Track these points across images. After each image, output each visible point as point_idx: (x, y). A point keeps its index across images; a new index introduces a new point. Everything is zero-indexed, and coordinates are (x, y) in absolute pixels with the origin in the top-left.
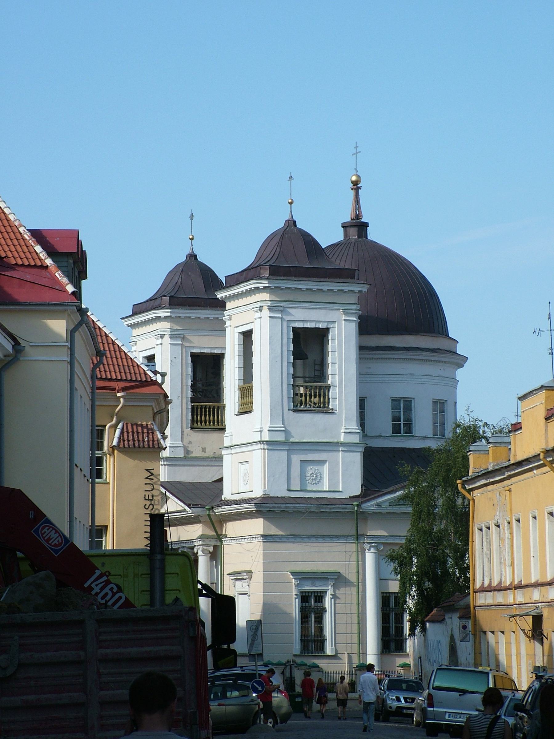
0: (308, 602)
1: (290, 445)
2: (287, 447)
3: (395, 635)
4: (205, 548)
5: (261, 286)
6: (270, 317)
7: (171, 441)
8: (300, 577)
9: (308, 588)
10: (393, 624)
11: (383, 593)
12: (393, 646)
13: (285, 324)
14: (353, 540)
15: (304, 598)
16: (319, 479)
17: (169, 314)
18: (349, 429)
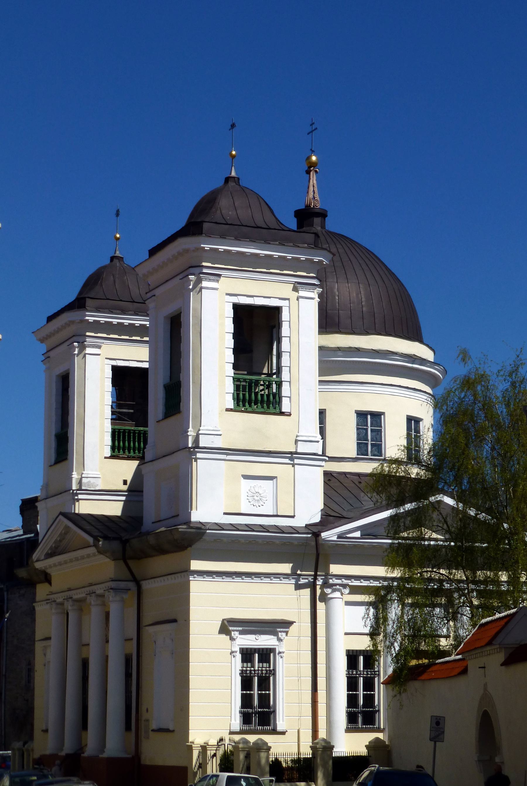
3: (364, 706)
11: (348, 651)
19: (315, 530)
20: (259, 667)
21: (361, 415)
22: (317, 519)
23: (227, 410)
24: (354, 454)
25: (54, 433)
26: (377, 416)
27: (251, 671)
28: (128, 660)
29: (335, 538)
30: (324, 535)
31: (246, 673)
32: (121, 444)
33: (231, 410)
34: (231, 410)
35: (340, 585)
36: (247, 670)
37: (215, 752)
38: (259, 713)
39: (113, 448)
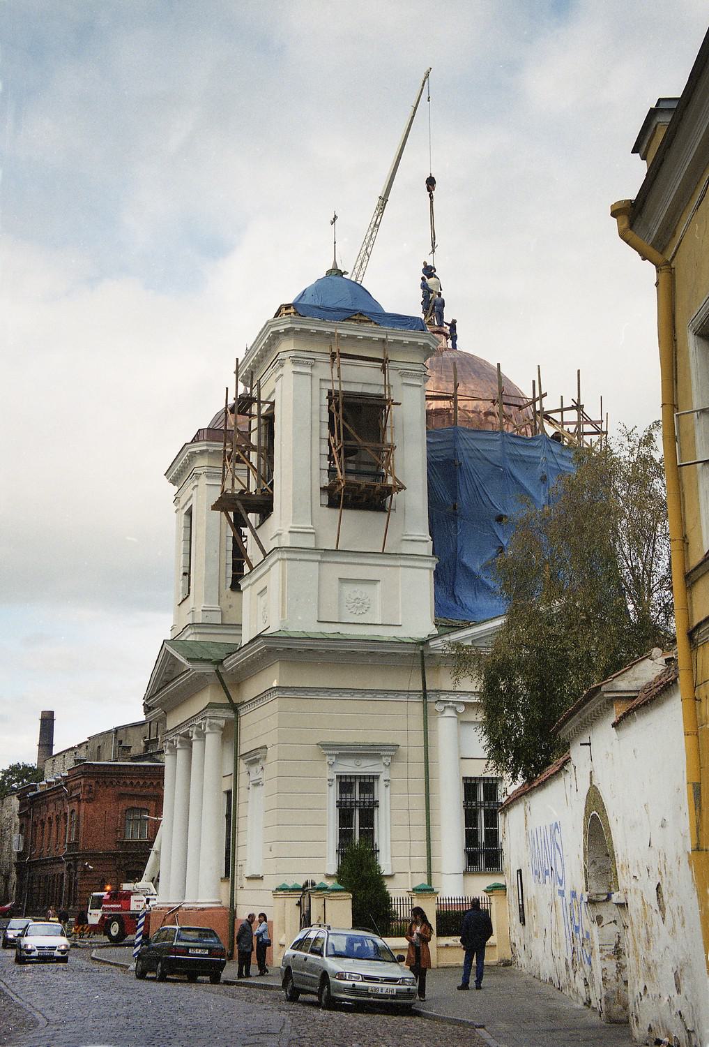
0: (351, 792)
1: (322, 555)
2: (318, 558)
4: (213, 721)
8: (337, 752)
9: (350, 767)
10: (482, 828)
11: (465, 779)
13: (316, 382)
14: (419, 698)
15: (345, 784)
16: (364, 605)
17: (205, 448)
36: (346, 802)
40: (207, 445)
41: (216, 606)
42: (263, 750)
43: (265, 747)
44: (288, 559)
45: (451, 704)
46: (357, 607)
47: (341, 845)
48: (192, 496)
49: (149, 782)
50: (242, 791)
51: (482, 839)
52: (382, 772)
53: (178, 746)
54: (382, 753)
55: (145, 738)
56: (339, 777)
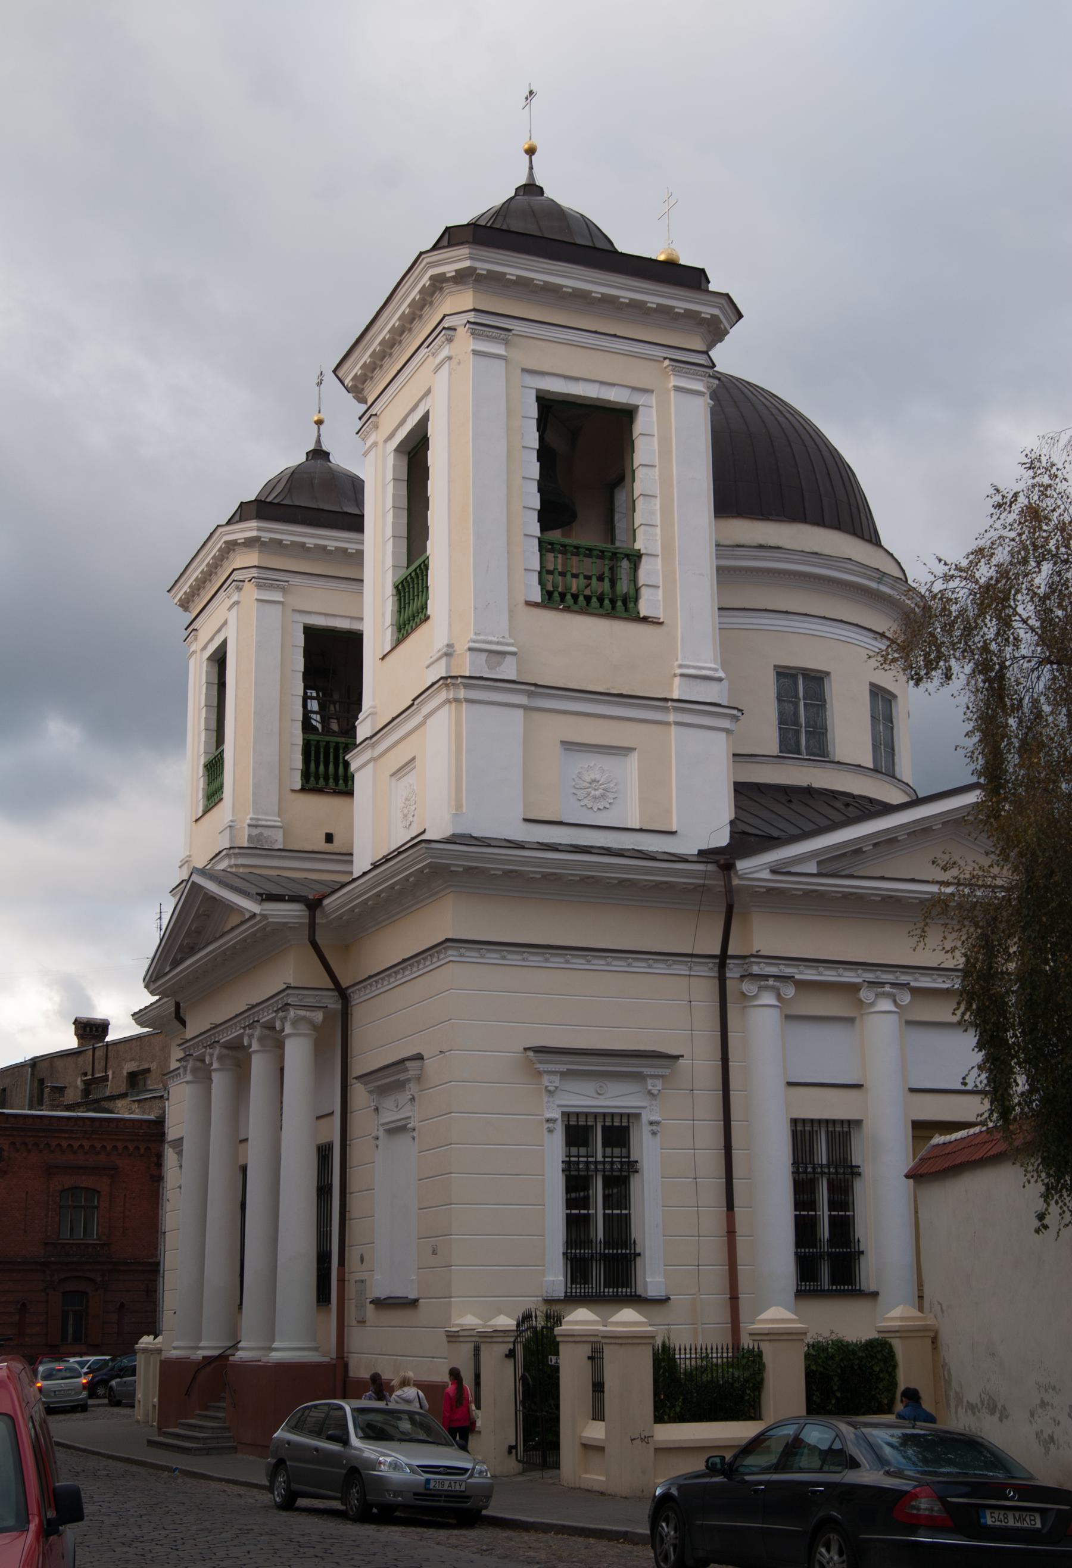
2: (523, 700)
3: (832, 1242)
4: (302, 1013)
5: (449, 270)
6: (476, 353)
7: (254, 813)
8: (563, 1068)
11: (795, 1122)
12: (825, 1271)
17: (254, 534)
18: (688, 667)
19: (721, 860)
20: (604, 1157)
21: (786, 675)
22: (722, 839)
23: (528, 603)
24: (774, 750)
25: (202, 761)
26: (816, 680)
27: (587, 1163)
28: (324, 1153)
29: (766, 875)
30: (742, 865)
31: (578, 1170)
32: (322, 768)
33: (536, 605)
34: (536, 605)
35: (776, 977)
36: (578, 1163)
37: (511, 1346)
38: (605, 1257)
39: (306, 775)
40: (259, 529)
41: (274, 820)
42: (417, 1063)
43: (419, 1057)
44: (468, 701)
45: (771, 982)
46: (595, 798)
47: (570, 1243)
48: (225, 623)
49: (99, 1146)
50: (358, 1150)
51: (825, 1231)
52: (645, 1108)
53: (215, 1065)
54: (646, 1071)
55: (85, 1074)
56: (566, 1115)
